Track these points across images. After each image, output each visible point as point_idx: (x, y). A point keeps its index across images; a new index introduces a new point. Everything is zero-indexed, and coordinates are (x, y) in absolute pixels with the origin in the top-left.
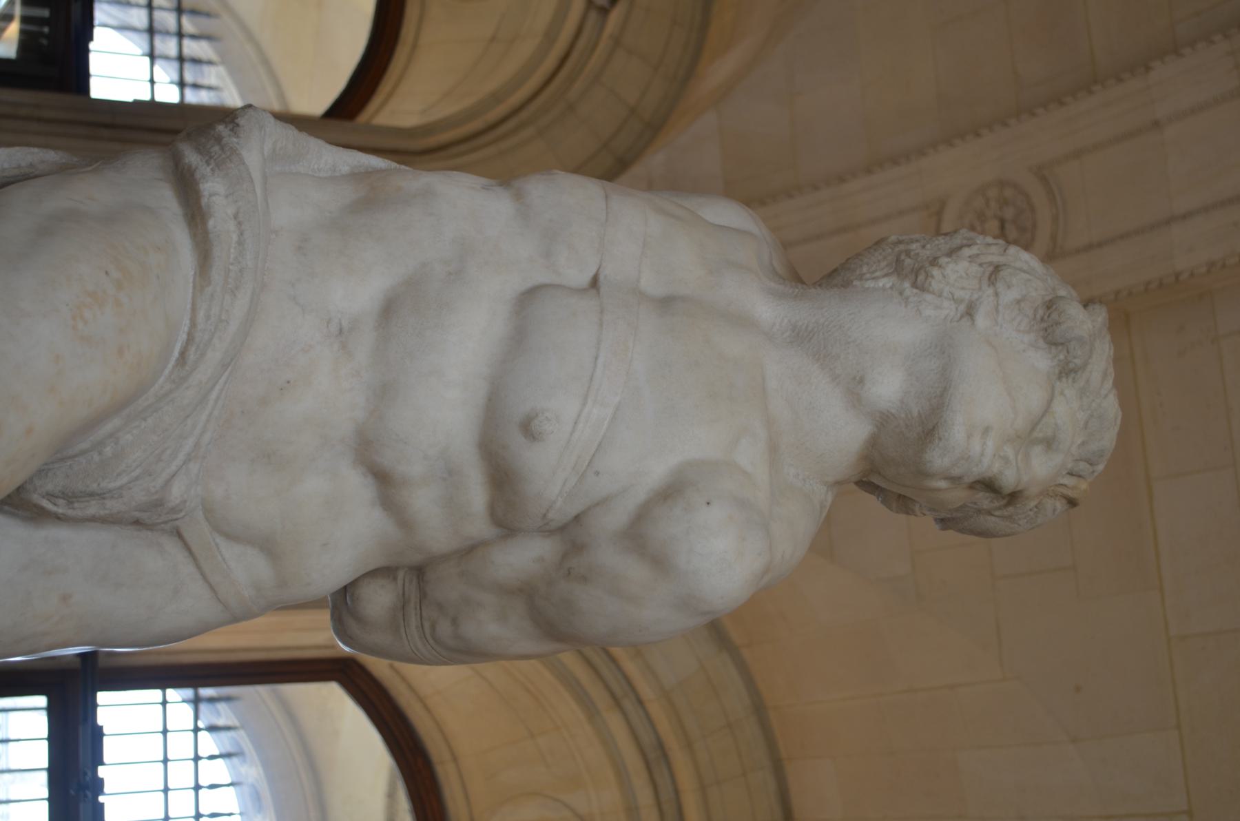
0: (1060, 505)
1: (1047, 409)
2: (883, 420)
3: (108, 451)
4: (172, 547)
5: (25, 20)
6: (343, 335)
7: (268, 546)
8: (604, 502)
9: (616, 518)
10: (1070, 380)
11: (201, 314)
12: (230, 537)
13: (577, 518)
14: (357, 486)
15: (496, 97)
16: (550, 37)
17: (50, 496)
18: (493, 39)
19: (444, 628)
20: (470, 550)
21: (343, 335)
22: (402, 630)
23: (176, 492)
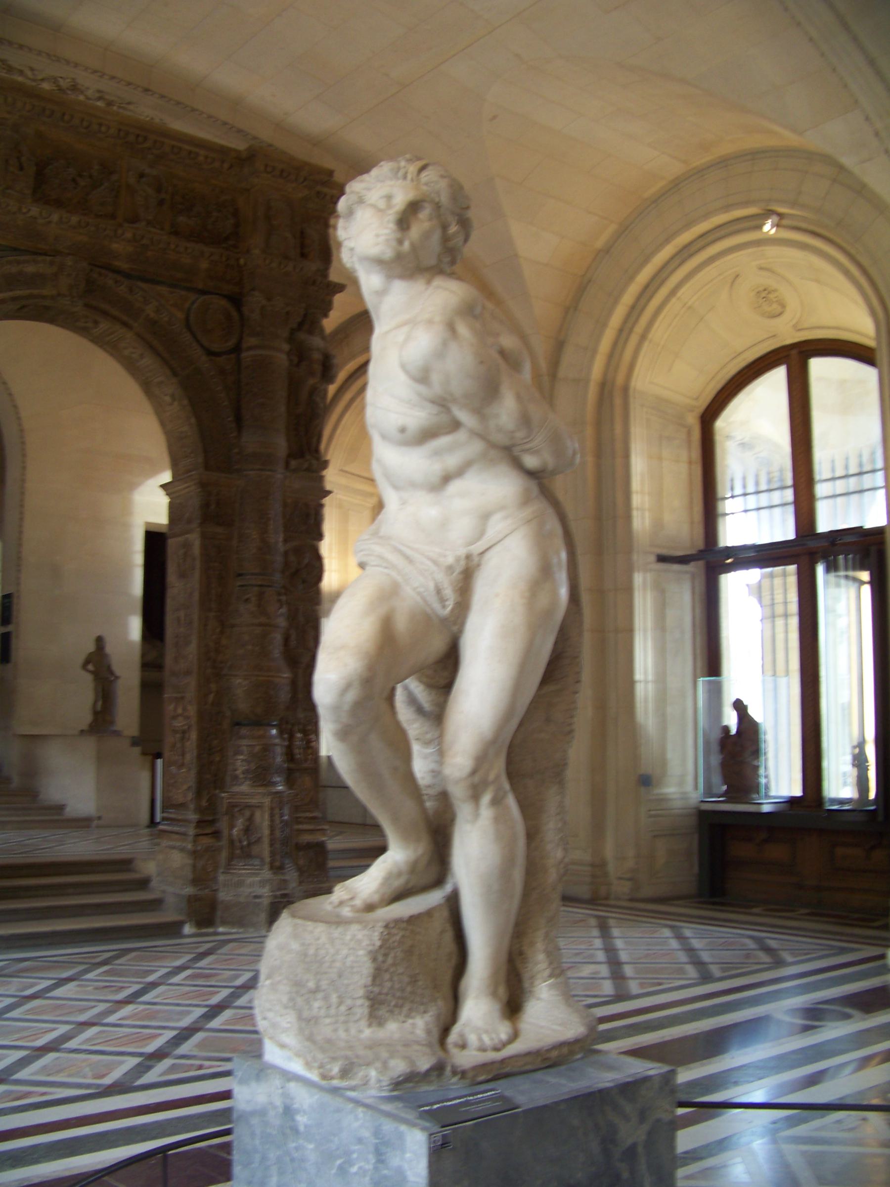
0: (424, 174)
1: (373, 206)
2: (390, 277)
3: (422, 590)
4: (488, 555)
5: (846, 569)
6: (404, 503)
7: (485, 517)
8: (419, 395)
9: (422, 389)
10: (364, 198)
11: (374, 563)
12: (482, 533)
13: (433, 402)
14: (455, 486)
15: (847, 273)
16: (803, 246)
17: (444, 607)
18: (817, 281)
19: (520, 435)
20: (475, 434)
21: (404, 503)
22: (536, 449)
23: (450, 560)
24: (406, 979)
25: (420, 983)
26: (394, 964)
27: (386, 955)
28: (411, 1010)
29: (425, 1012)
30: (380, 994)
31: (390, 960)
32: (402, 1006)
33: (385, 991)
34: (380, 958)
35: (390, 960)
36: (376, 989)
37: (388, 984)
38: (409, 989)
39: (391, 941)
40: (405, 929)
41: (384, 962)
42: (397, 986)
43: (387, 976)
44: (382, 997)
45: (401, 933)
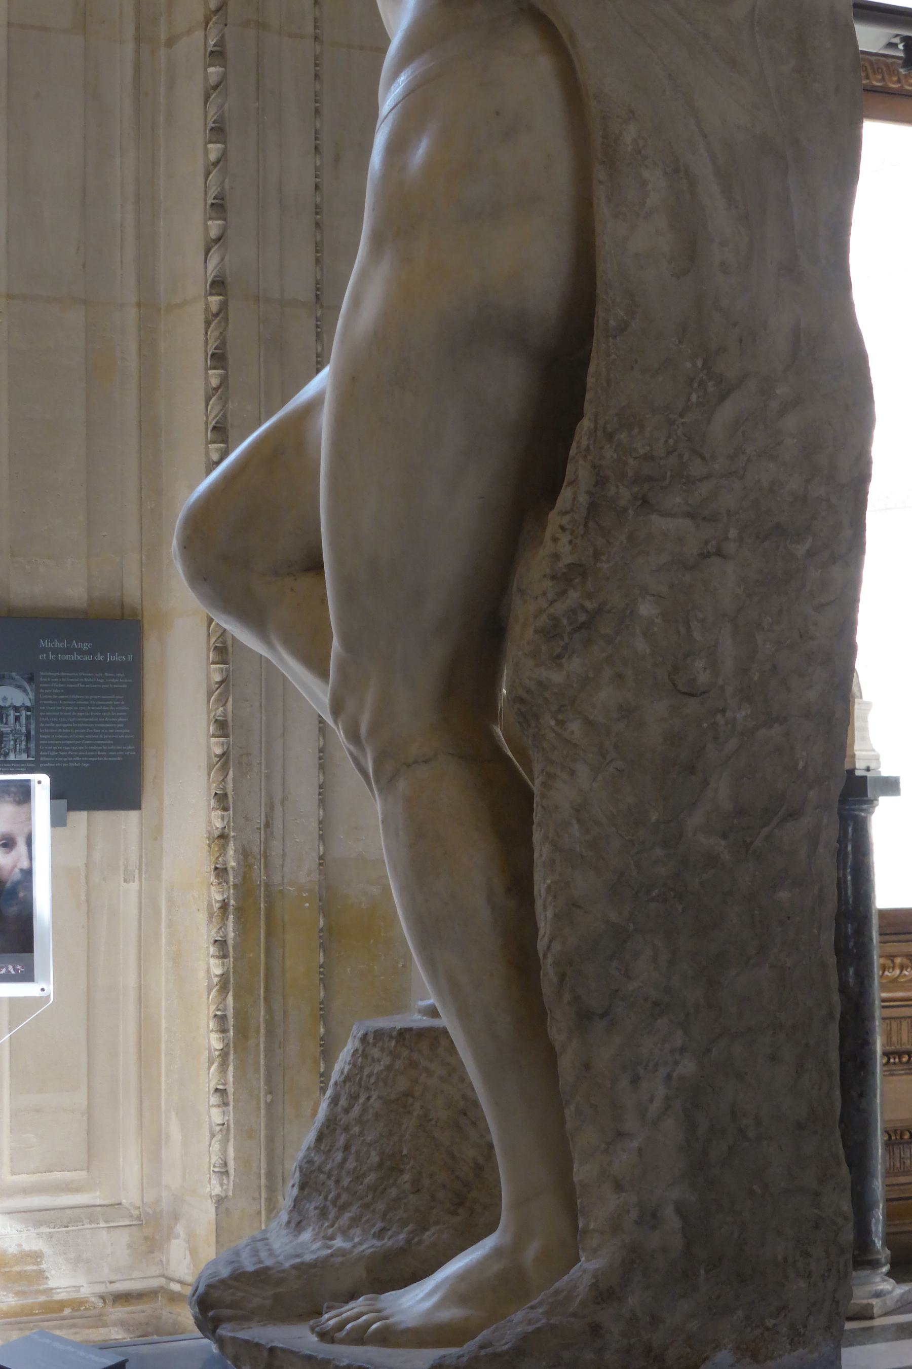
24: (374, 1158)
25: (406, 1177)
26: (359, 1120)
27: (354, 1098)
28: (355, 1221)
29: (380, 1235)
30: (320, 1170)
31: (356, 1111)
32: (343, 1208)
33: (329, 1166)
34: (343, 1102)
35: (356, 1111)
36: (318, 1159)
37: (339, 1156)
38: (371, 1178)
39: (366, 1072)
40: (395, 1056)
41: (347, 1111)
42: (351, 1164)
43: (342, 1140)
44: (322, 1177)
45: (387, 1060)
